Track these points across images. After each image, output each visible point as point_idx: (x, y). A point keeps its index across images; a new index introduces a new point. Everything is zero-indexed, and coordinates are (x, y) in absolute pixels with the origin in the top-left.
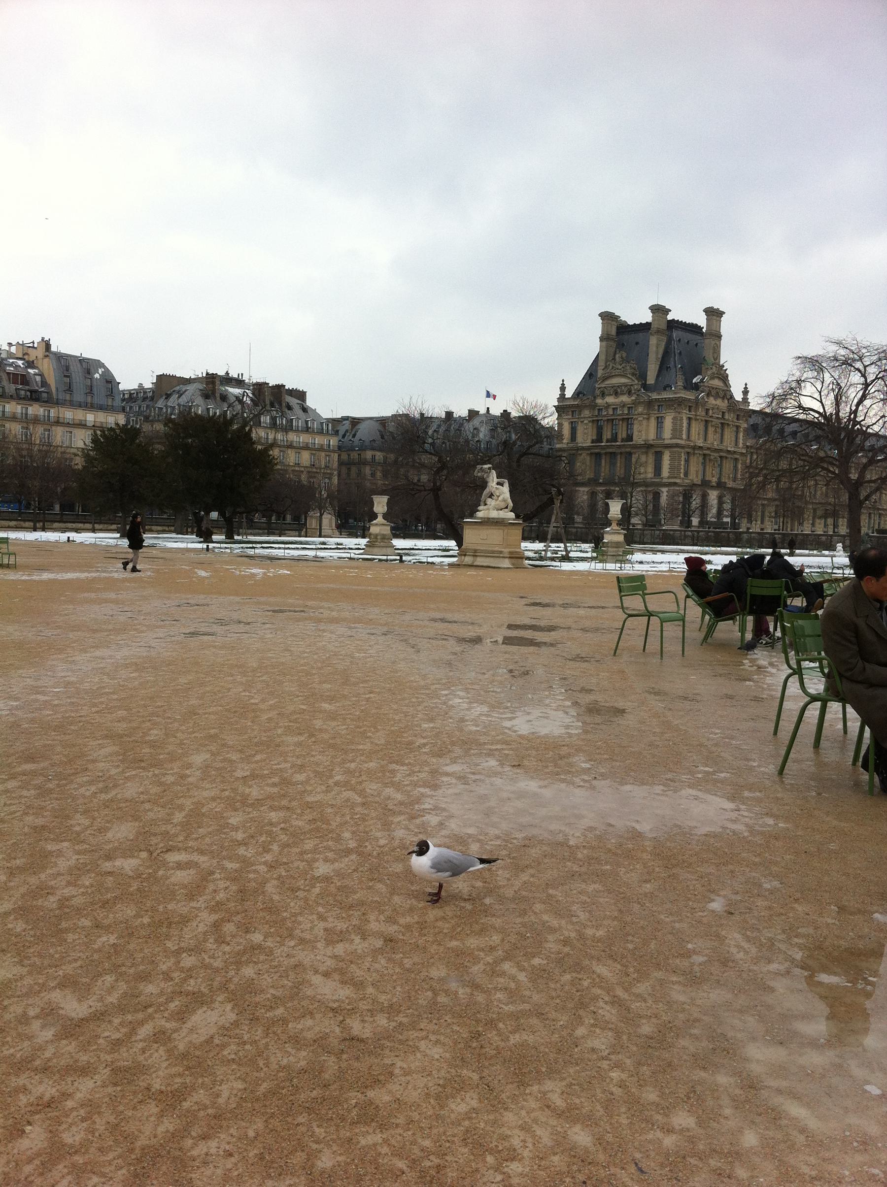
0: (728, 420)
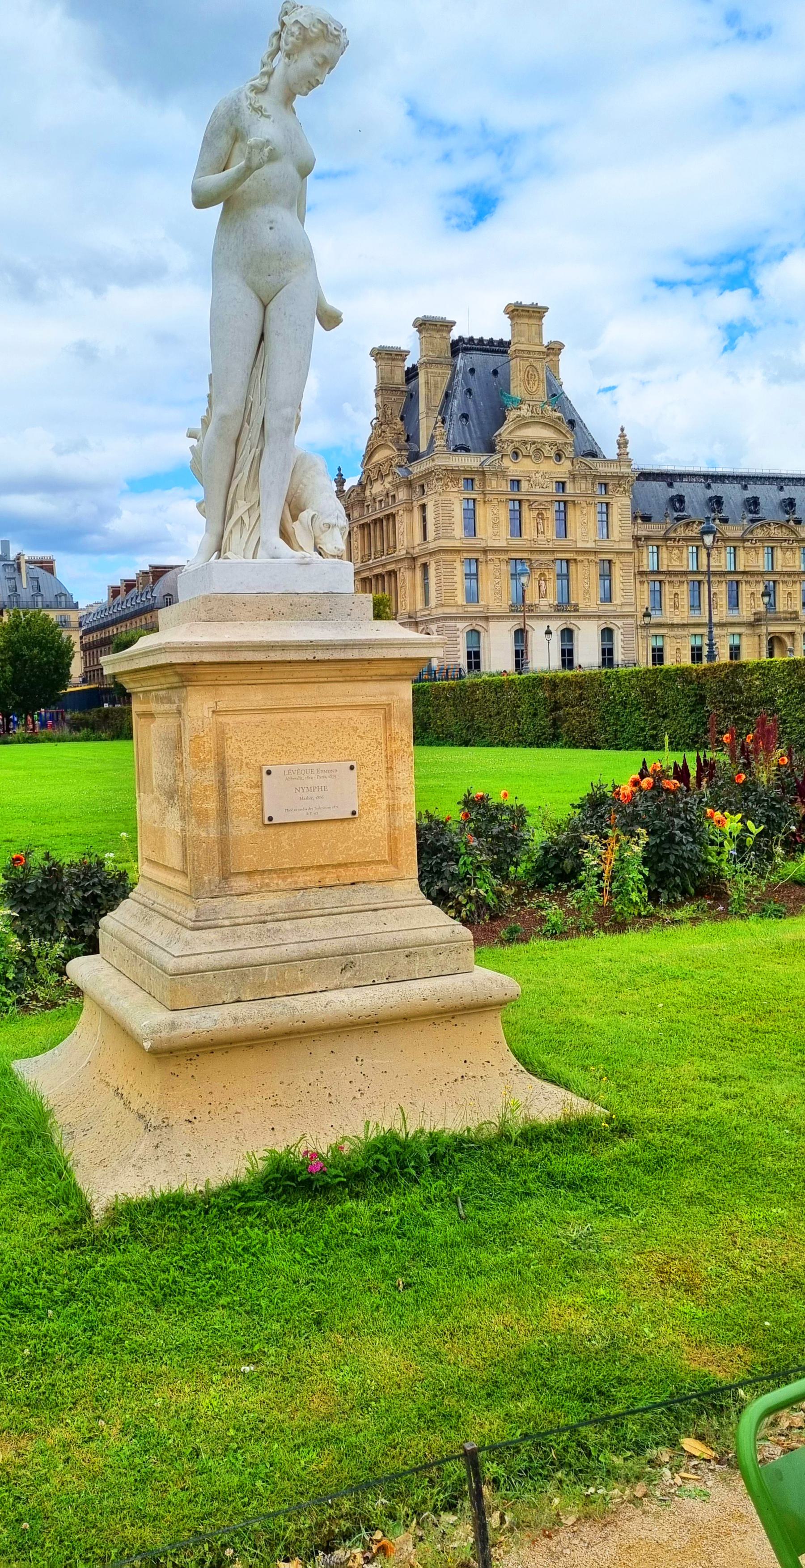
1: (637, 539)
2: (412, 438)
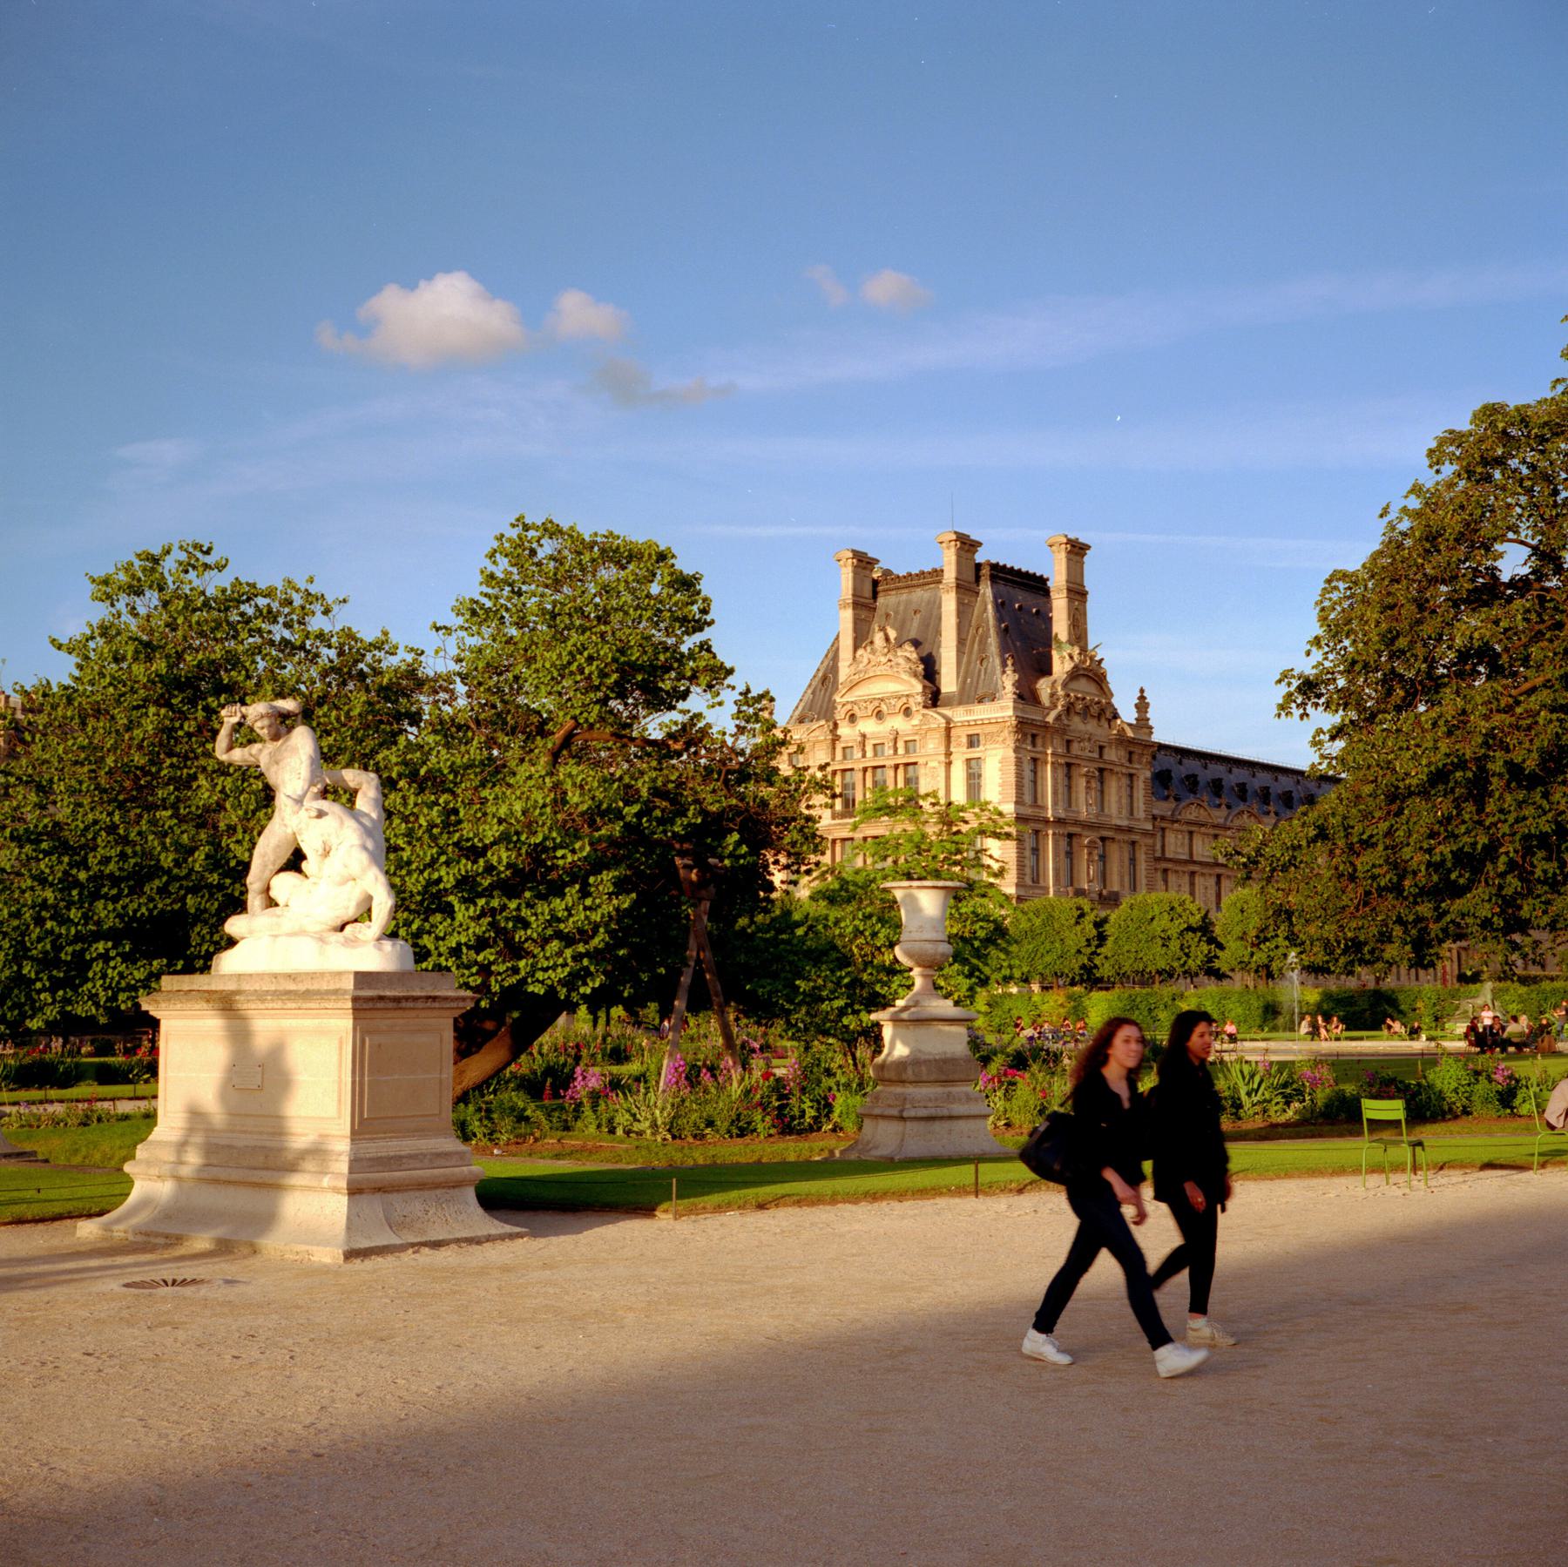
0: (1112, 763)
1: (1154, 818)
2: (930, 671)
